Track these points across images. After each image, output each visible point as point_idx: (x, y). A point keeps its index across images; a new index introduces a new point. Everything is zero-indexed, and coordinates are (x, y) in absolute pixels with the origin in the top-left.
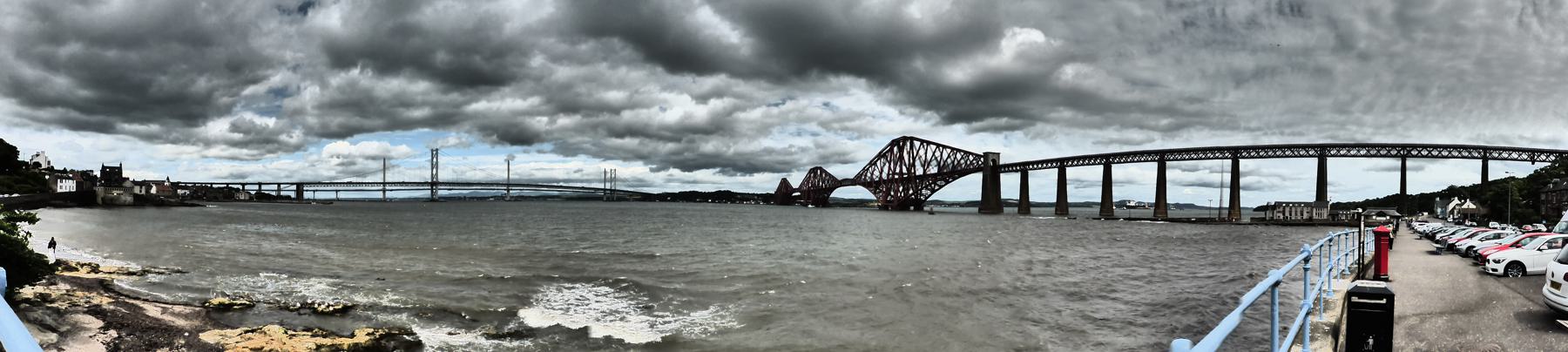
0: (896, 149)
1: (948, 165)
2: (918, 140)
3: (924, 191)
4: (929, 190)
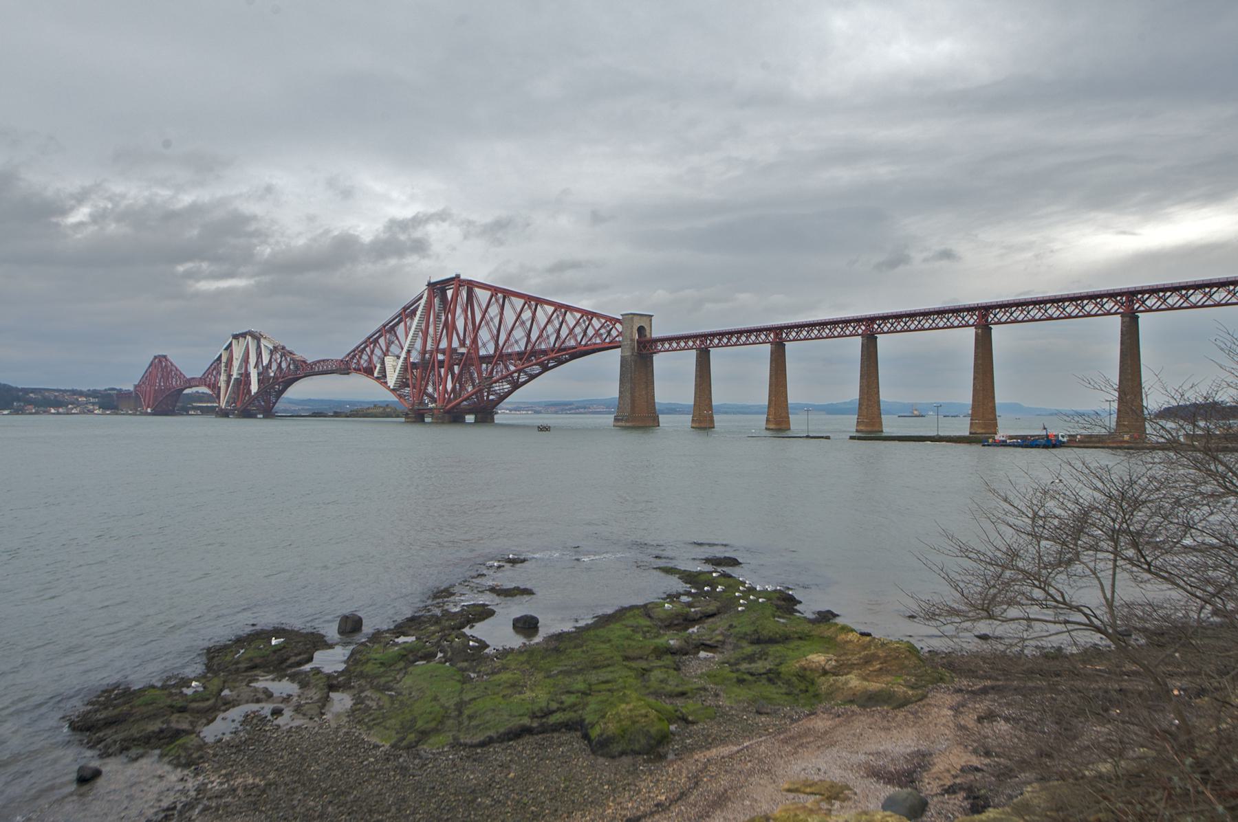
1: (548, 337)
3: (496, 387)
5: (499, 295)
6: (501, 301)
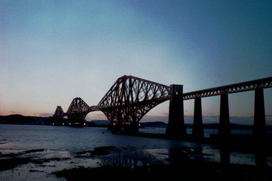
0: (121, 86)
2: (133, 77)
4: (139, 113)
5: (137, 81)
6: (138, 83)
